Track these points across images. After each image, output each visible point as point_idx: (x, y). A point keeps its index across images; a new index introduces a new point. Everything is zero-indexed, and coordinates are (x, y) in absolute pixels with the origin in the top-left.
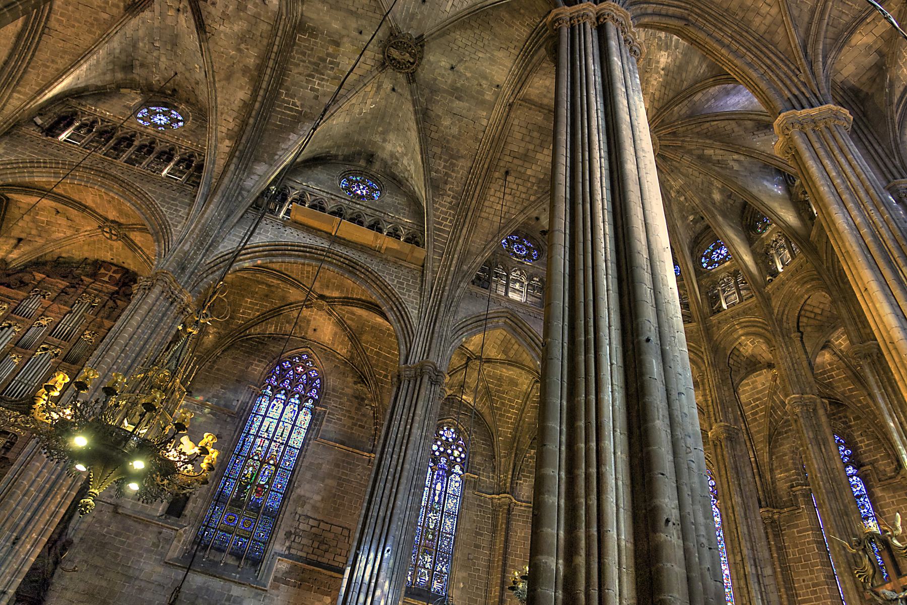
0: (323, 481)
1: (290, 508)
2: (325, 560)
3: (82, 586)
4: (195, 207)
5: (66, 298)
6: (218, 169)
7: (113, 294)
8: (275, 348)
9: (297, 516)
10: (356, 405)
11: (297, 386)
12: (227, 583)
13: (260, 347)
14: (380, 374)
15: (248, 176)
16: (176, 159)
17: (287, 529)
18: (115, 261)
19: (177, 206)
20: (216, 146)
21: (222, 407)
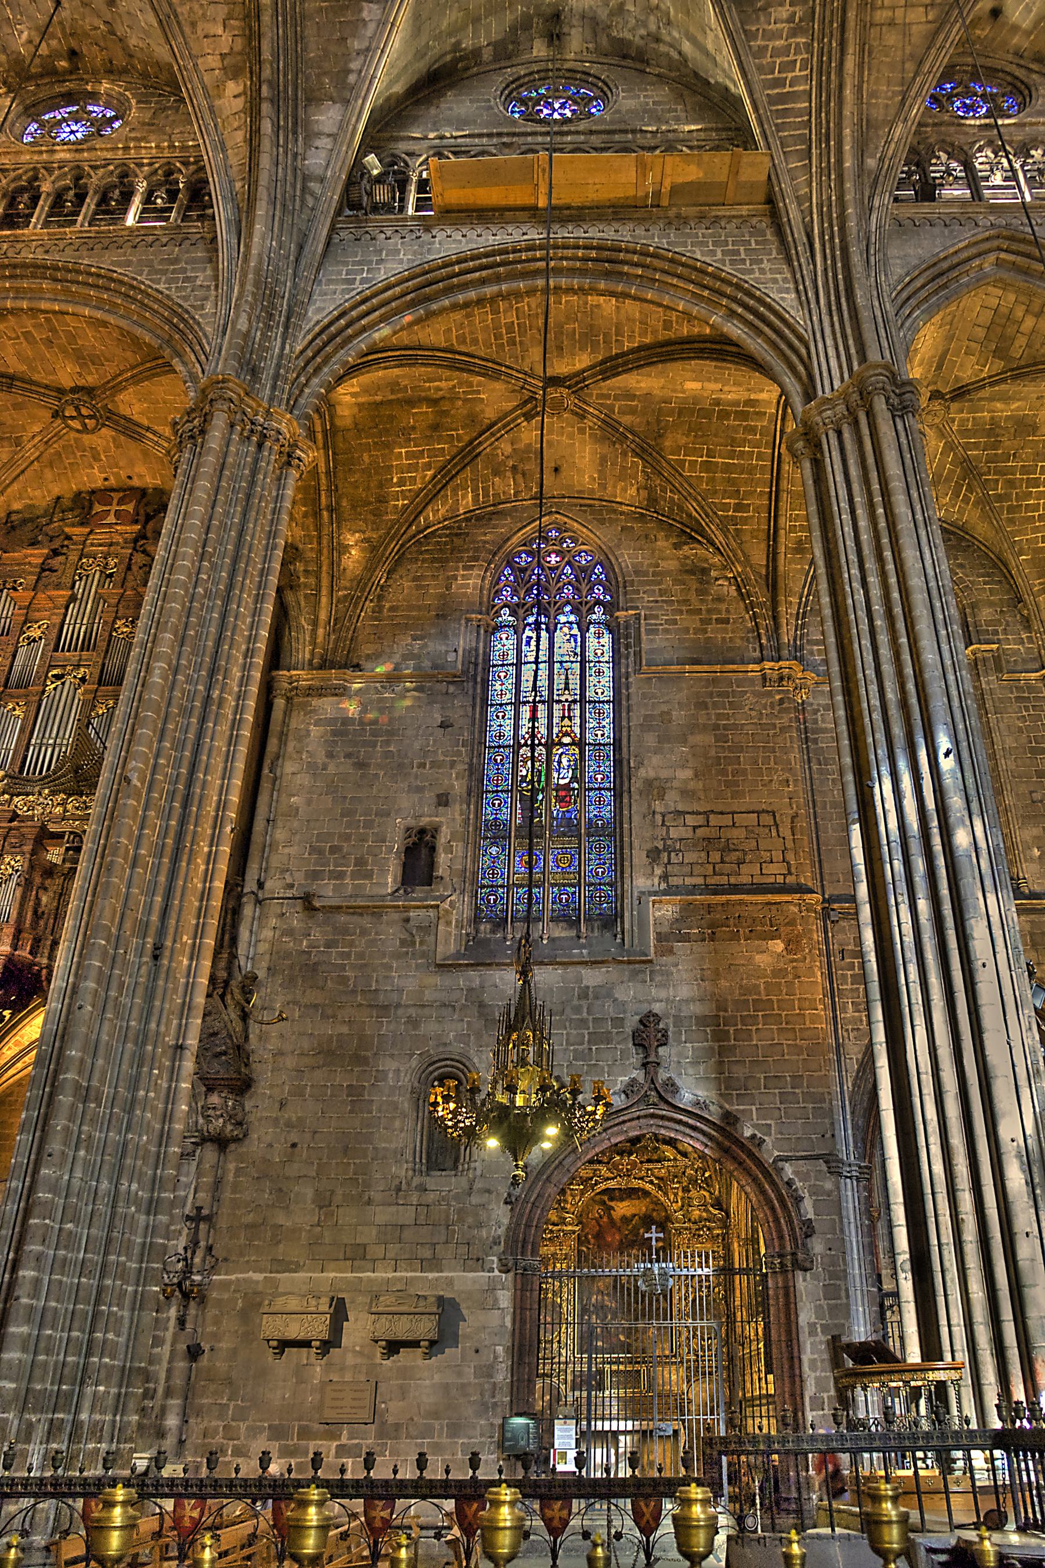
0: (684, 741)
1: (637, 808)
2: (745, 879)
3: (306, 1044)
4: (223, 255)
5: (54, 578)
6: (237, 157)
7: (135, 541)
8: (488, 536)
9: (659, 818)
10: (695, 586)
11: (560, 590)
12: (570, 969)
13: (457, 541)
14: (726, 507)
15: (307, 145)
16: (142, 186)
17: (649, 846)
18: (113, 482)
19: (185, 271)
20: (211, 109)
21: (430, 671)
